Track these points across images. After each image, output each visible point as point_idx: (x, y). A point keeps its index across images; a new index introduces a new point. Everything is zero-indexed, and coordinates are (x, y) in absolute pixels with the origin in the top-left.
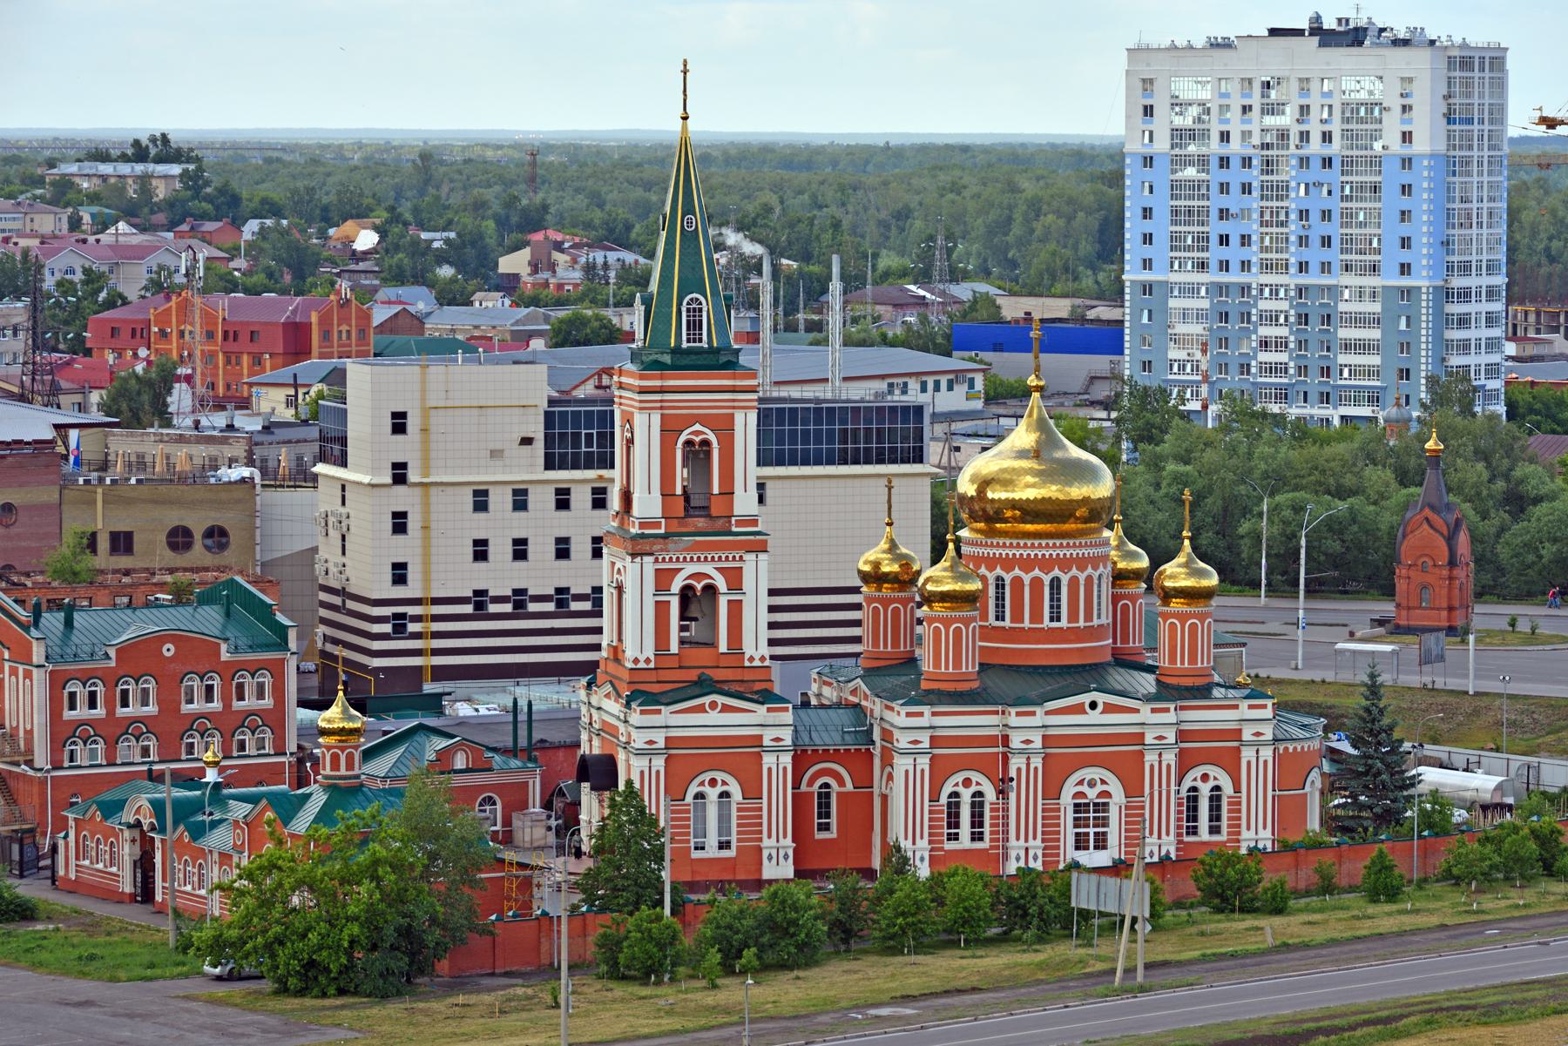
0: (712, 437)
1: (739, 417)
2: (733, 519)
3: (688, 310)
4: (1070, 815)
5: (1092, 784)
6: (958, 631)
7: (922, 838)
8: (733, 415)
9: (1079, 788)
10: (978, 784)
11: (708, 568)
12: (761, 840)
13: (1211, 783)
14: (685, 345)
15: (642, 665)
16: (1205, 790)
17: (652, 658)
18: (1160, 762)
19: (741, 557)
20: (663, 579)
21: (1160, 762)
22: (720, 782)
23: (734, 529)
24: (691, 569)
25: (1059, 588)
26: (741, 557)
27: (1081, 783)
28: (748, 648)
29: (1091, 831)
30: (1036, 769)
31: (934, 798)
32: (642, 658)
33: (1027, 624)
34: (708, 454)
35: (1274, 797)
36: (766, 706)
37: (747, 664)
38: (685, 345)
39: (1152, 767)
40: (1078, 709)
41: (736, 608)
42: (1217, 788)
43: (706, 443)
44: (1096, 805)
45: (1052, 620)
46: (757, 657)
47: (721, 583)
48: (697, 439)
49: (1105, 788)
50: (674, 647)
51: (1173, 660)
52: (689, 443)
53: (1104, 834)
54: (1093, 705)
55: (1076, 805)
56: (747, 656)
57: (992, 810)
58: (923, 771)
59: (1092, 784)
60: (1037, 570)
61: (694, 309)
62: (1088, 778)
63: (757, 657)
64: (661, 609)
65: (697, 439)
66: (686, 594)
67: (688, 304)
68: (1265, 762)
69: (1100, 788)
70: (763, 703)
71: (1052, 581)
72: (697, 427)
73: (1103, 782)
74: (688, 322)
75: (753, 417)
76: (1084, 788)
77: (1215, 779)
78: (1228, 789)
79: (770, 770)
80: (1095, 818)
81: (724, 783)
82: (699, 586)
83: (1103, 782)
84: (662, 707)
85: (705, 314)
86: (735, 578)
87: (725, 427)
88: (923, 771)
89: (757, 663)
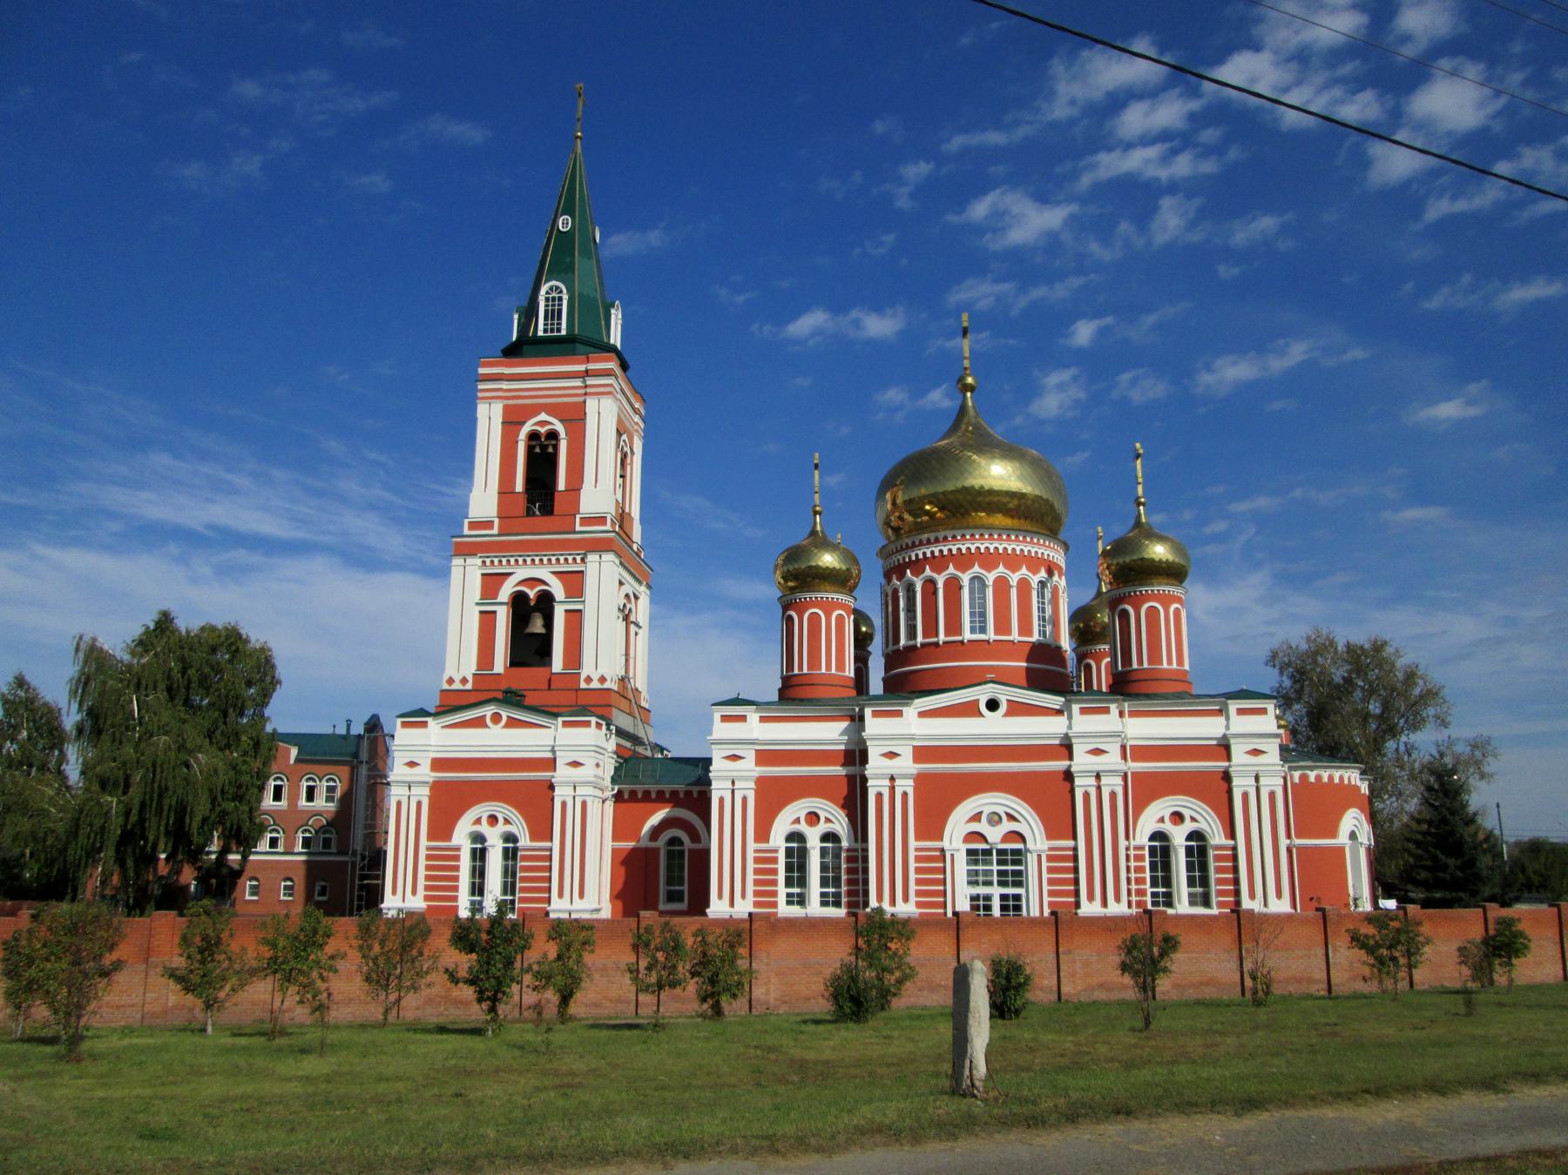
0: (559, 427)
1: (591, 404)
2: (578, 517)
3: (547, 299)
4: (961, 866)
5: (995, 819)
7: (743, 896)
9: (975, 827)
10: (828, 820)
11: (543, 573)
12: (549, 901)
13: (1188, 827)
15: (457, 686)
16: (1179, 837)
17: (470, 678)
18: (1099, 788)
20: (492, 583)
21: (1099, 788)
22: (501, 820)
24: (522, 573)
27: (977, 817)
28: (587, 669)
29: (996, 891)
30: (905, 794)
31: (763, 834)
32: (457, 678)
34: (556, 447)
35: (1289, 851)
36: (560, 720)
37: (583, 685)
38: (540, 333)
39: (1086, 796)
40: (970, 710)
41: (575, 618)
42: (1196, 836)
43: (553, 435)
44: (1000, 852)
45: (973, 630)
46: (595, 677)
47: (557, 589)
48: (543, 430)
49: (1013, 826)
50: (500, 663)
52: (533, 436)
53: (1017, 897)
54: (993, 705)
55: (970, 852)
56: (583, 677)
57: (849, 860)
58: (745, 800)
59: (995, 819)
61: (554, 299)
62: (987, 810)
63: (595, 677)
64: (488, 619)
65: (543, 430)
66: (518, 600)
67: (547, 293)
68: (1272, 795)
69: (1007, 826)
70: (555, 715)
71: (972, 579)
72: (543, 417)
73: (1011, 818)
74: (546, 312)
76: (982, 827)
77: (1193, 819)
78: (1217, 837)
79: (564, 804)
80: (1000, 873)
81: (507, 821)
82: (532, 594)
83: (1011, 818)
84: (429, 720)
85: (565, 303)
86: (574, 583)
87: (575, 417)
88: (745, 800)
89: (595, 685)
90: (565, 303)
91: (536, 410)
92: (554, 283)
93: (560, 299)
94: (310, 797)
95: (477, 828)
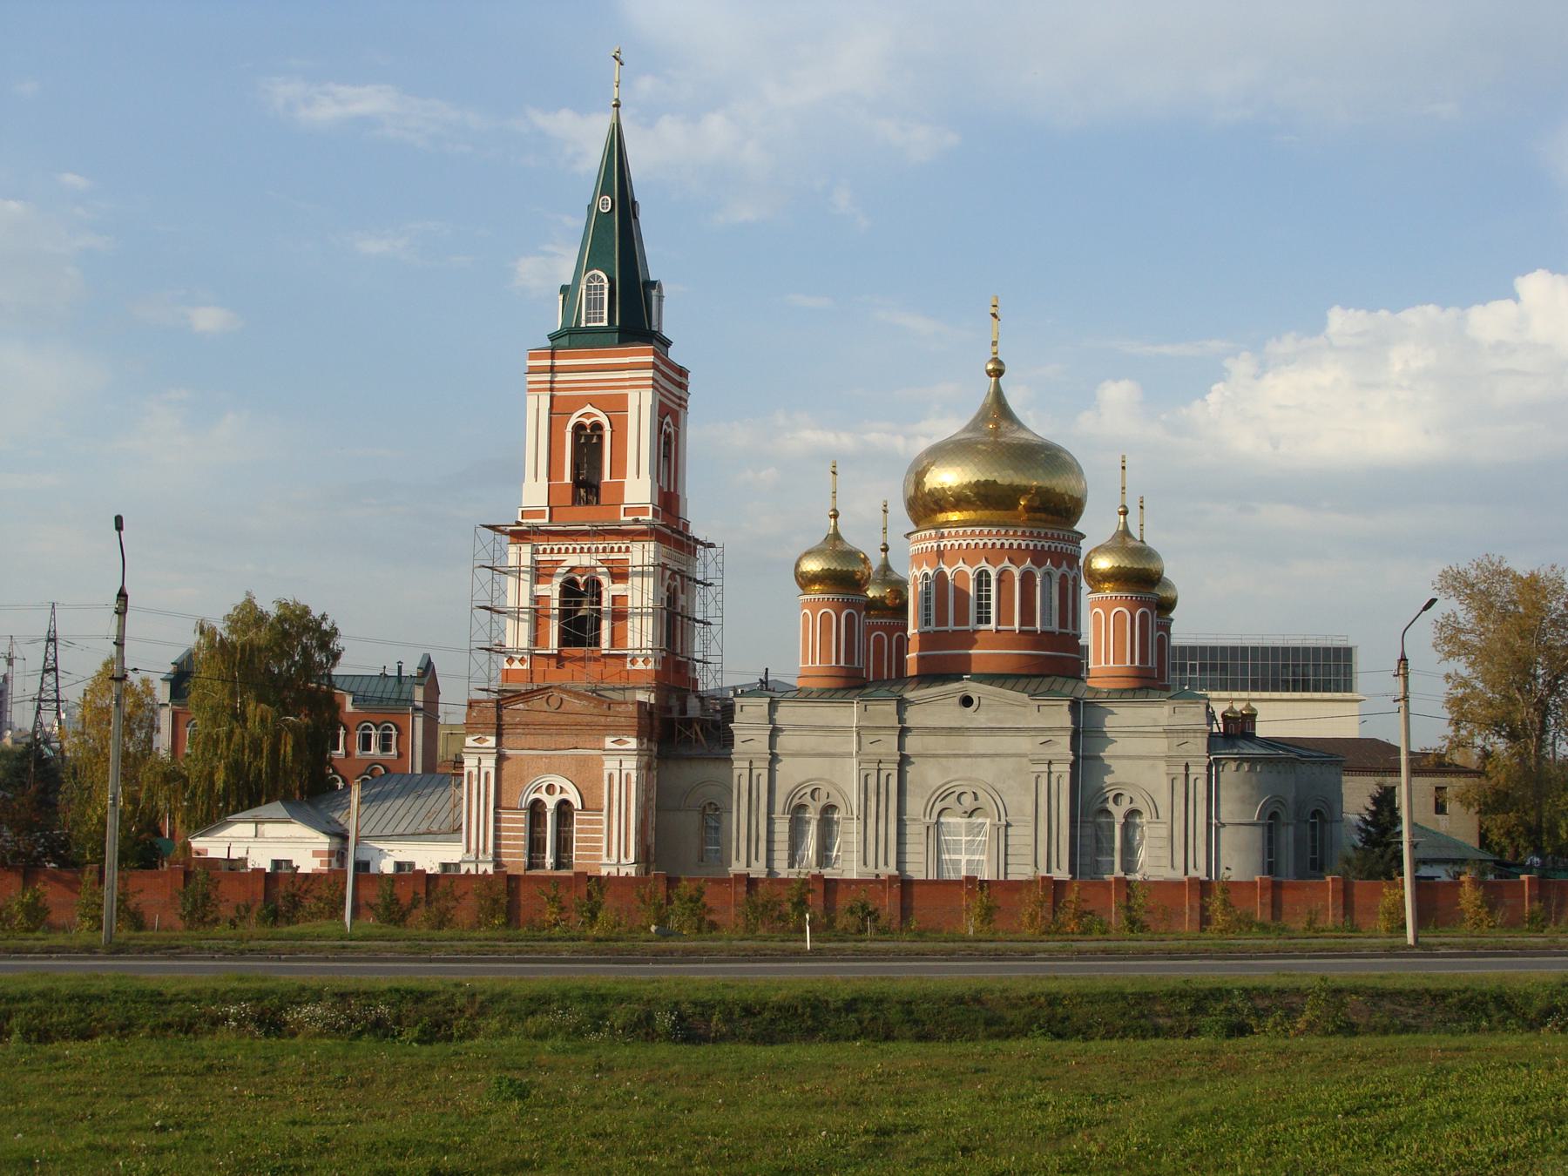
0: (604, 420)
1: (633, 396)
3: (588, 288)
6: (879, 639)
8: (627, 395)
14: (583, 325)
19: (627, 548)
23: (623, 518)
25: (988, 584)
26: (627, 548)
33: (951, 626)
34: (601, 438)
38: (583, 325)
43: (597, 427)
48: (588, 422)
51: (1098, 661)
52: (579, 428)
60: (961, 563)
65: (588, 422)
67: (589, 281)
71: (980, 575)
72: (589, 409)
75: (648, 396)
82: (581, 580)
87: (616, 406)
90: (606, 292)
91: (580, 402)
92: (595, 272)
93: (602, 288)
94: (366, 746)
95: (537, 796)
